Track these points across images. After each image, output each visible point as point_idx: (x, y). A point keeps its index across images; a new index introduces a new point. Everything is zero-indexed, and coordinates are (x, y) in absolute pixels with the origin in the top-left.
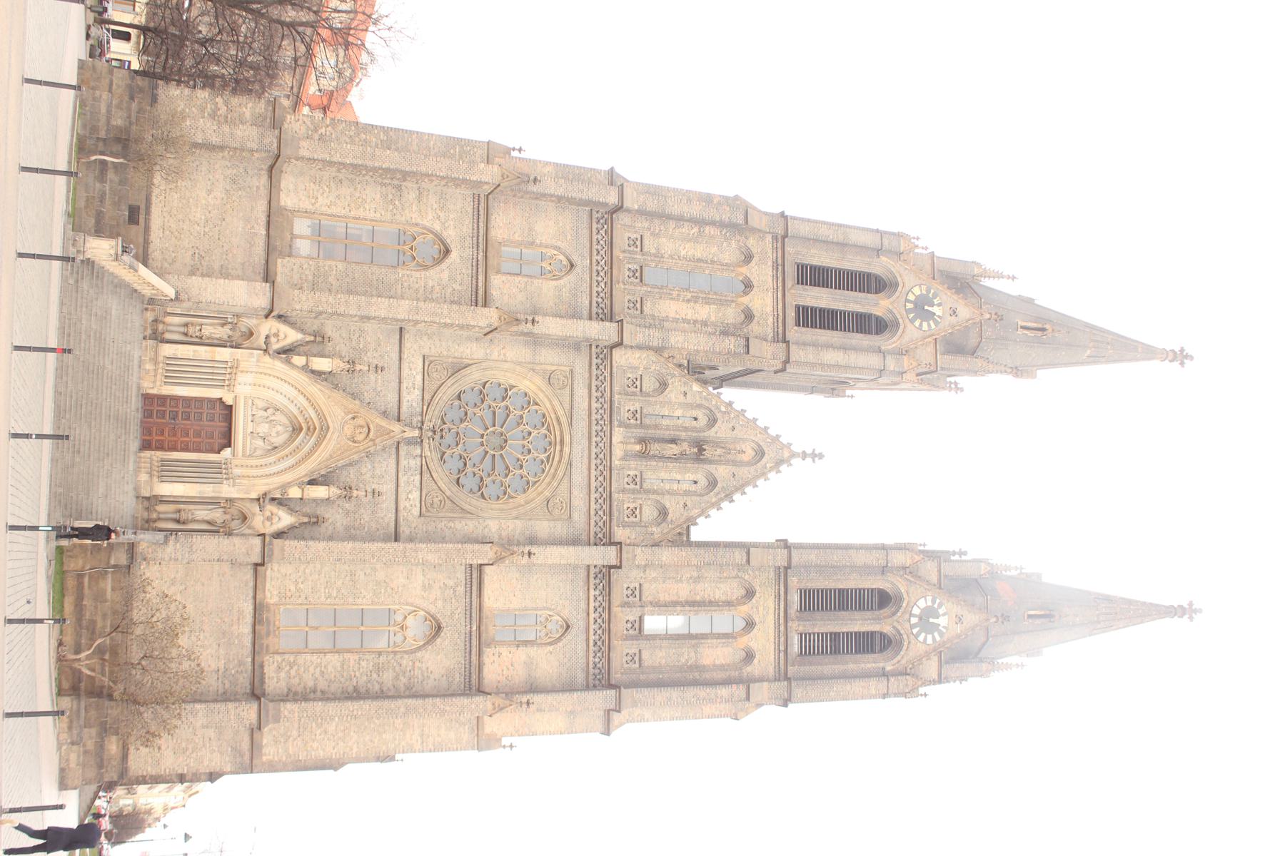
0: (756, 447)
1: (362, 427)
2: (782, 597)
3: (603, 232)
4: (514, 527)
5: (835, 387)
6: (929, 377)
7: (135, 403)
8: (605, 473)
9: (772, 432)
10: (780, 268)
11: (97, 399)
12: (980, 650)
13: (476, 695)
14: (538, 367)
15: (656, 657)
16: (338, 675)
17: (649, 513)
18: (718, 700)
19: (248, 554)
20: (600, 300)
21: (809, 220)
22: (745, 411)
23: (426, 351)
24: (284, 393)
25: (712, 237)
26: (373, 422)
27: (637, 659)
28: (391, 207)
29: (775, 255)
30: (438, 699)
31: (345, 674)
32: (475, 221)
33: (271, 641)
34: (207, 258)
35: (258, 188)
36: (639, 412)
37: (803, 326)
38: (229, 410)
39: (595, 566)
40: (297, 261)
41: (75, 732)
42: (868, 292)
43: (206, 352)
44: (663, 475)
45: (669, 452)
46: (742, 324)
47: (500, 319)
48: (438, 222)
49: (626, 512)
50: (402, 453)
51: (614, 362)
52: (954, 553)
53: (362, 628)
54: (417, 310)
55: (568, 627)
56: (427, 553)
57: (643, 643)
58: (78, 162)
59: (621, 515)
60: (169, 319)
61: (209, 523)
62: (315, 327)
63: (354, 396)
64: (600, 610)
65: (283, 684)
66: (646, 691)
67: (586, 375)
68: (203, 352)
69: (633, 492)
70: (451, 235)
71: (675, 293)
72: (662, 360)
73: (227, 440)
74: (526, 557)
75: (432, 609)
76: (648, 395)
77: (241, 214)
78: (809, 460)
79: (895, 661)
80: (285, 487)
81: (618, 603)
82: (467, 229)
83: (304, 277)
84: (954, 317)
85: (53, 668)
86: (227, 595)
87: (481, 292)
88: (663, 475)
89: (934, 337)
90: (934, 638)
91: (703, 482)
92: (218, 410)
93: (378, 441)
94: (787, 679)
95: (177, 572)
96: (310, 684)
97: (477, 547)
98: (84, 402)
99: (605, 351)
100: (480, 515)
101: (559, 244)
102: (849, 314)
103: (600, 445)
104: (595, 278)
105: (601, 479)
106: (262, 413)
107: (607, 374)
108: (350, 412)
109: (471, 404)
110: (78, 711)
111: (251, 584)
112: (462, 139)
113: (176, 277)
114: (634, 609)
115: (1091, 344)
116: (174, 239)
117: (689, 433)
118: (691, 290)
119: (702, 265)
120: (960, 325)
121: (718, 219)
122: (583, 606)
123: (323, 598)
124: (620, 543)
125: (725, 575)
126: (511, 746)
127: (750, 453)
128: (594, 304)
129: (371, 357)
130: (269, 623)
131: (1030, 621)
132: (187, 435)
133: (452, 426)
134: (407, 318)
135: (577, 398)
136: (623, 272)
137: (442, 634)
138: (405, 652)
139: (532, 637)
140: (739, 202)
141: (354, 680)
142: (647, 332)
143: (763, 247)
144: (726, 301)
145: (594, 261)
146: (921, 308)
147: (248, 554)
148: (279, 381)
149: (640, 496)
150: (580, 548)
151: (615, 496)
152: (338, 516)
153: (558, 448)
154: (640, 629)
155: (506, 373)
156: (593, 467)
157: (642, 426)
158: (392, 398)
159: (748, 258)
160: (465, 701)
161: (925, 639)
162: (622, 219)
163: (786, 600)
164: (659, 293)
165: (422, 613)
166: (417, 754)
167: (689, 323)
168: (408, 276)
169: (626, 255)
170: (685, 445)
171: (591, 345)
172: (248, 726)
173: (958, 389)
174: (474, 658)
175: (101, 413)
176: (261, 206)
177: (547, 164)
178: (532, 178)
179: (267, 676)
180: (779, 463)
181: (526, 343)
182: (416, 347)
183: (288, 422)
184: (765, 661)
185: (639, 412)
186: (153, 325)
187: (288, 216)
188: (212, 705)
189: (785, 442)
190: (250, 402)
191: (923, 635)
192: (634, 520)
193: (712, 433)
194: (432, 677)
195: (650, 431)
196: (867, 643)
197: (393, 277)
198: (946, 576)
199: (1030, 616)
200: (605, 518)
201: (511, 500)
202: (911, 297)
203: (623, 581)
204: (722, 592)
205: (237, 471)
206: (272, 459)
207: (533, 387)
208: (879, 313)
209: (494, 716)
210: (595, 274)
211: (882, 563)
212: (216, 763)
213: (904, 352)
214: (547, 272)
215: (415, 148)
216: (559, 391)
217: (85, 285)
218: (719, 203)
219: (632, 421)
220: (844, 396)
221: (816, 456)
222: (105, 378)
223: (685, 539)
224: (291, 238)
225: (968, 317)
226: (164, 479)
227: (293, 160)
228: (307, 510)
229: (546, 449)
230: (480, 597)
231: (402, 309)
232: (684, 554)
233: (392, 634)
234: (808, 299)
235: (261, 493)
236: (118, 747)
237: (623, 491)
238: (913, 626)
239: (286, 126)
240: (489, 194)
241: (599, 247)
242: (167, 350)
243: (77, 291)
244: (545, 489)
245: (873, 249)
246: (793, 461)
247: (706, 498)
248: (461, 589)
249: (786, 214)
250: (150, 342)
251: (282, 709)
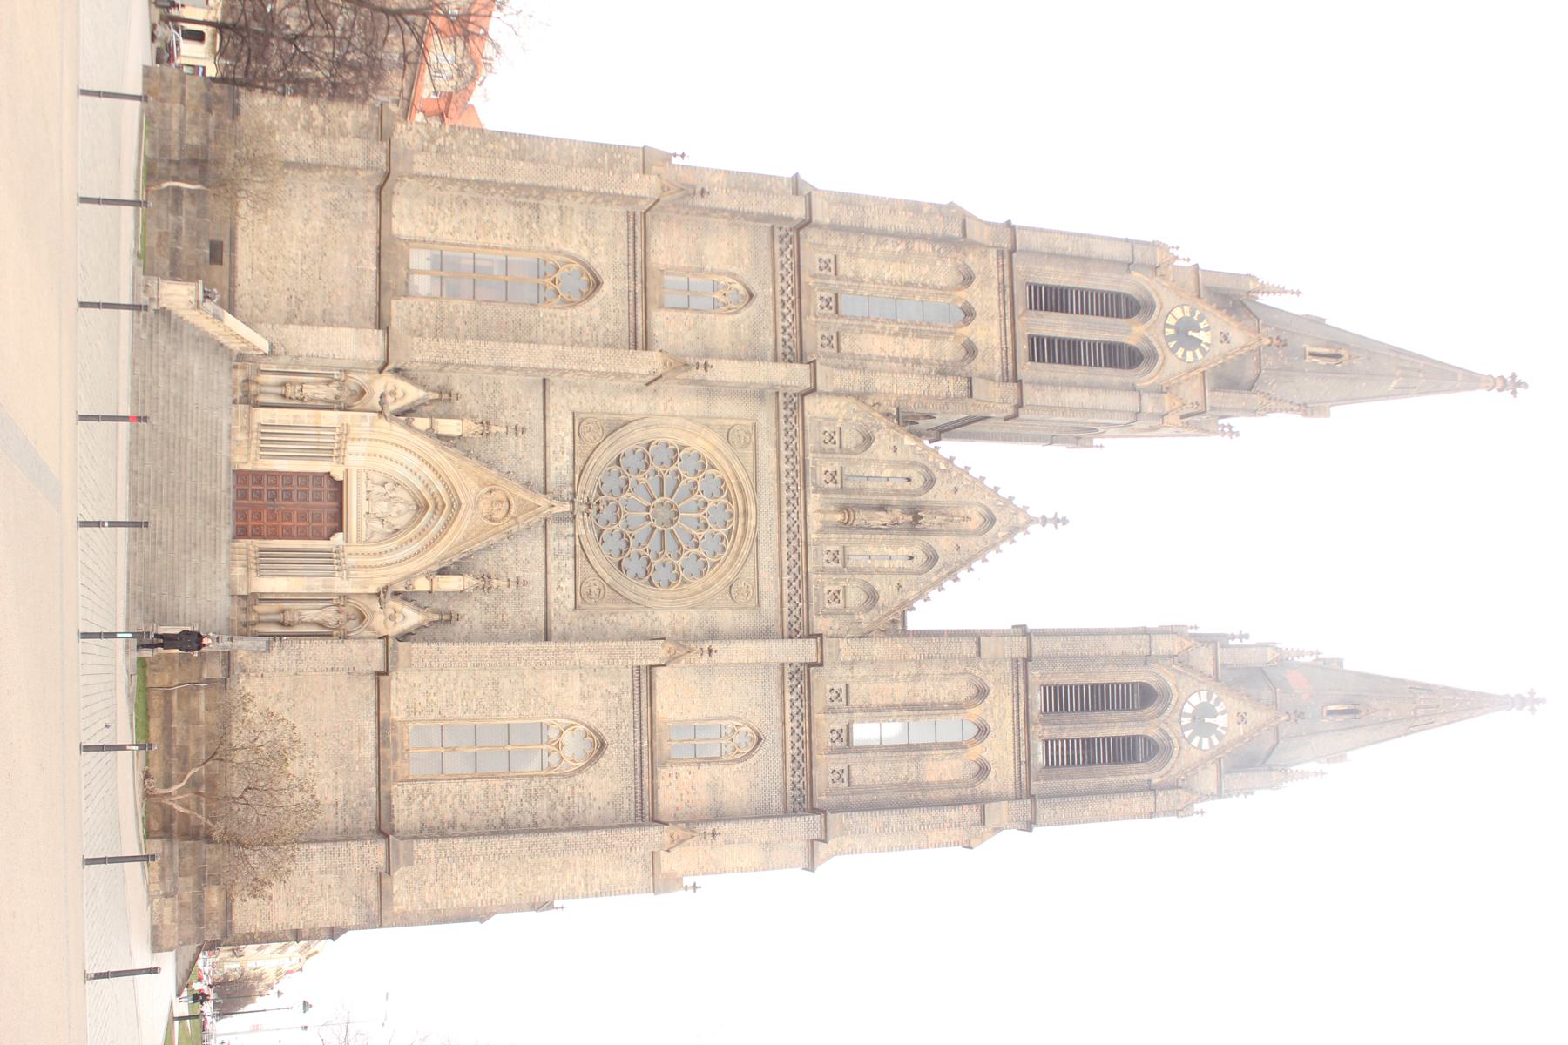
0: (984, 512)
1: (501, 502)
2: (1022, 696)
3: (787, 253)
4: (690, 619)
5: (1080, 436)
6: (1196, 419)
7: (226, 482)
9: (1003, 493)
10: (1008, 290)
11: (180, 477)
12: (1268, 755)
13: (649, 826)
14: (713, 423)
15: (869, 773)
16: (481, 805)
17: (855, 597)
18: (947, 825)
19: (367, 660)
20: (787, 337)
21: (1041, 230)
22: (969, 468)
23: (576, 407)
24: (405, 464)
26: (514, 496)
27: (845, 776)
28: (527, 232)
29: (1001, 275)
30: (604, 832)
31: (490, 804)
32: (631, 245)
33: (399, 766)
34: (306, 303)
35: (365, 214)
36: (839, 473)
37: (1039, 361)
38: (339, 487)
39: (791, 665)
40: (416, 302)
41: (168, 881)
42: (1117, 317)
43: (308, 416)
44: (871, 550)
45: (877, 522)
46: (963, 360)
47: (665, 364)
48: (585, 248)
49: (827, 597)
50: (551, 532)
51: (806, 413)
52: (1233, 637)
53: (509, 748)
54: (564, 357)
55: (760, 739)
56: (585, 653)
57: (852, 757)
58: (147, 191)
59: (821, 601)
60: (263, 378)
61: (319, 624)
62: (440, 382)
63: (490, 464)
64: (798, 717)
65: (415, 818)
66: (858, 816)
67: (774, 430)
68: (305, 416)
69: (835, 571)
70: (601, 264)
71: (879, 326)
72: (865, 408)
73: (338, 524)
74: (706, 655)
75: (594, 723)
76: (849, 452)
77: (346, 247)
78: (1050, 526)
79: (1164, 771)
80: (409, 578)
81: (821, 708)
82: (621, 254)
83: (424, 321)
84: (1225, 344)
85: (139, 804)
86: (344, 712)
87: (640, 332)
88: (871, 550)
89: (1201, 370)
90: (1211, 743)
91: (920, 557)
92: (326, 486)
93: (521, 518)
94: (1031, 796)
95: (283, 685)
96: (448, 817)
97: (646, 644)
98: (165, 481)
99: (795, 399)
101: (734, 269)
102: (1094, 345)
103: (792, 515)
104: (779, 310)
105: (794, 556)
106: (379, 489)
107: (798, 428)
108: (485, 485)
109: (633, 470)
110: (171, 856)
111: (373, 698)
112: (611, 145)
113: (270, 326)
114: (840, 716)
115: (1398, 372)
116: (265, 280)
117: (902, 498)
118: (899, 320)
119: (911, 289)
120: (1233, 354)
121: (929, 233)
122: (778, 712)
123: (460, 713)
124: (821, 635)
125: (951, 670)
126: (695, 887)
127: (976, 521)
128: (780, 343)
129: (509, 417)
130: (396, 746)
131: (1331, 718)
132: (290, 519)
133: (610, 498)
135: (763, 459)
136: (814, 301)
137: (607, 752)
138: (560, 775)
139: (716, 753)
140: (953, 211)
141: (502, 811)
142: (845, 374)
143: (986, 265)
144: (942, 333)
145: (778, 289)
146: (1184, 335)
147: (367, 660)
148: (399, 449)
149: (844, 577)
150: (772, 642)
151: (813, 577)
153: (741, 520)
154: (848, 741)
155: (675, 431)
156: (785, 543)
157: (843, 490)
158: (537, 465)
159: (968, 279)
160: (637, 832)
161: (1200, 743)
162: (811, 237)
163: (1026, 700)
164: (859, 326)
165: (581, 727)
166: (580, 900)
167: (897, 362)
168: (551, 316)
169: (817, 280)
170: (897, 513)
171: (777, 393)
172: (375, 869)
173: (1233, 433)
174: (646, 780)
175: (185, 495)
176: (370, 237)
177: (717, 171)
178: (699, 189)
179: (395, 809)
180: (1013, 531)
181: (698, 393)
182: (563, 401)
183: (410, 499)
184: (1003, 776)
185: (839, 473)
186: (243, 387)
187: (402, 247)
188: (330, 846)
189: (1020, 506)
190: (364, 474)
191: (1197, 738)
192: (837, 605)
193: (929, 496)
194: (596, 805)
195: (853, 497)
196: (1125, 751)
198: (1224, 665)
199: (1330, 713)
200: (801, 604)
201: (685, 586)
202: (1171, 321)
203: (826, 682)
204: (947, 691)
205: (351, 561)
206: (393, 545)
207: (709, 448)
209: (673, 851)
210: (779, 305)
211: (1144, 650)
212: (338, 916)
213: (1164, 390)
214: (721, 305)
215: (554, 157)
216: (739, 451)
217: (161, 340)
218: (930, 213)
219: (831, 485)
220: (1092, 446)
222: (188, 453)
223: (900, 627)
224: (408, 274)
225: (1243, 343)
226: (264, 572)
227: (406, 179)
228: (438, 605)
229: (726, 523)
230: (651, 706)
231: (544, 357)
232: (899, 646)
233: (545, 754)
234: (1044, 328)
236: (220, 899)
237: (823, 571)
238: (1185, 728)
239: (396, 136)
240: (647, 211)
241: (784, 272)
242: (262, 415)
243: (151, 348)
244: (726, 572)
245: (1122, 263)
246: (1031, 528)
247: (924, 576)
248: (628, 697)
249: (1013, 223)
250: (241, 407)
251: (415, 848)
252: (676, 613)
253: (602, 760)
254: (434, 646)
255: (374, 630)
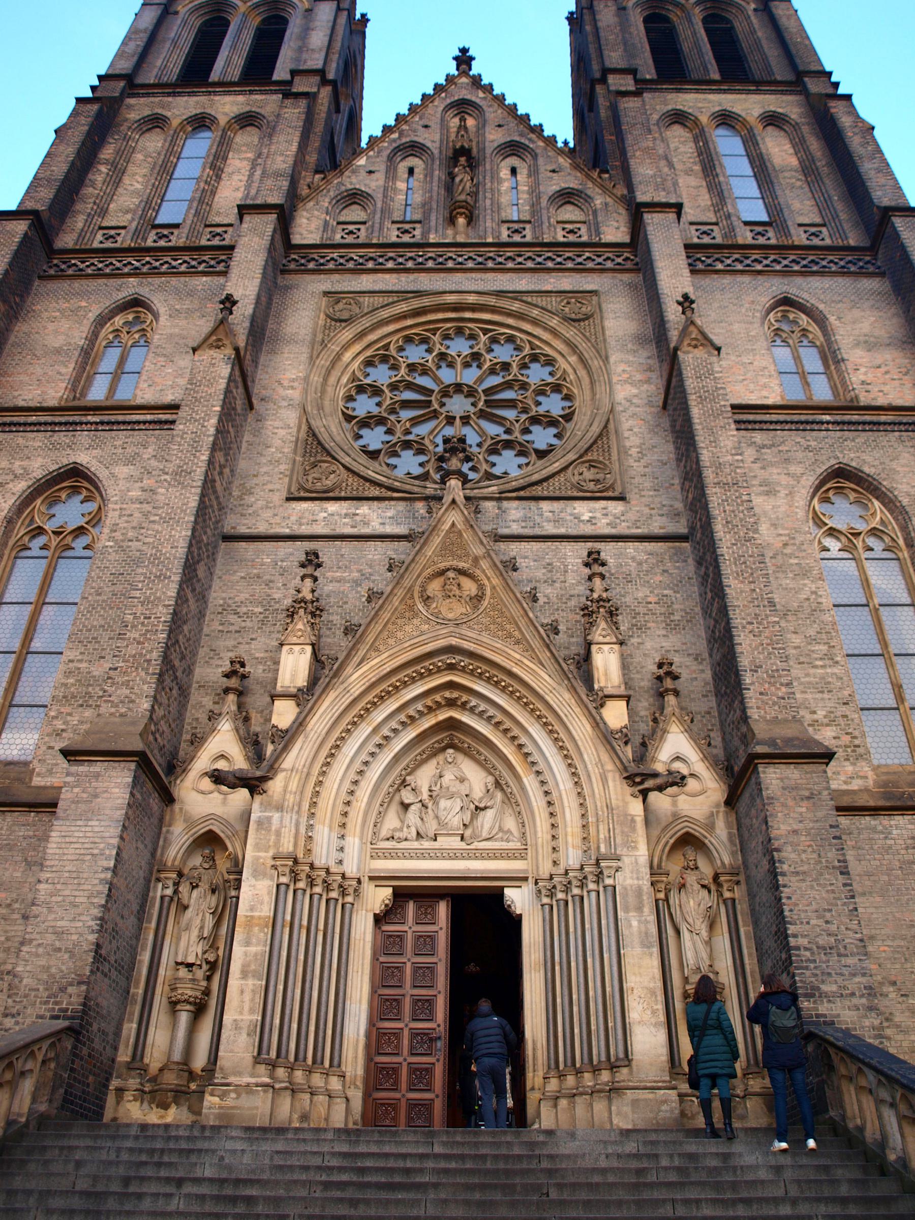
8: (509, 254)
17: (569, 213)
19: (808, 798)
23: (278, 498)
25: (119, 152)
27: (813, 230)
45: (468, 184)
47: (218, 347)
48: (11, 485)
55: (786, 302)
61: (711, 926)
75: (810, 480)
80: (606, 736)
82: (36, 440)
86: (886, 878)
91: (513, 161)
100: (607, 408)
101: (92, 316)
106: (413, 816)
108: (411, 608)
109: (388, 438)
122: (746, 279)
134: (199, 490)
137: (854, 464)
152: (648, 645)
153: (468, 315)
165: (816, 500)
181: (273, 352)
183: (433, 763)
197: (113, 556)
200: (587, 254)
206: (530, 782)
207: (357, 348)
208: (259, 19)
221: (464, 59)
226: (617, 1050)
232: (638, 153)
235: (628, 790)
247: (538, 151)
248: (759, 437)
252: (615, 379)
253: (866, 469)
254: (747, 679)
255: (712, 814)
